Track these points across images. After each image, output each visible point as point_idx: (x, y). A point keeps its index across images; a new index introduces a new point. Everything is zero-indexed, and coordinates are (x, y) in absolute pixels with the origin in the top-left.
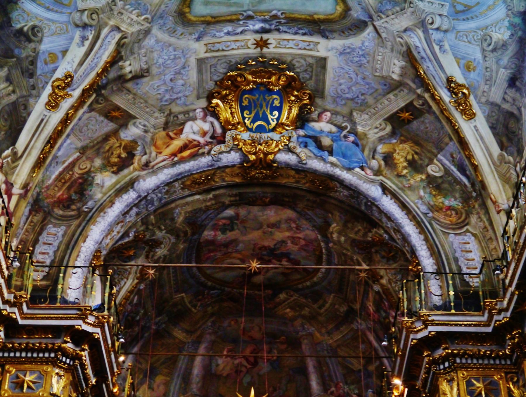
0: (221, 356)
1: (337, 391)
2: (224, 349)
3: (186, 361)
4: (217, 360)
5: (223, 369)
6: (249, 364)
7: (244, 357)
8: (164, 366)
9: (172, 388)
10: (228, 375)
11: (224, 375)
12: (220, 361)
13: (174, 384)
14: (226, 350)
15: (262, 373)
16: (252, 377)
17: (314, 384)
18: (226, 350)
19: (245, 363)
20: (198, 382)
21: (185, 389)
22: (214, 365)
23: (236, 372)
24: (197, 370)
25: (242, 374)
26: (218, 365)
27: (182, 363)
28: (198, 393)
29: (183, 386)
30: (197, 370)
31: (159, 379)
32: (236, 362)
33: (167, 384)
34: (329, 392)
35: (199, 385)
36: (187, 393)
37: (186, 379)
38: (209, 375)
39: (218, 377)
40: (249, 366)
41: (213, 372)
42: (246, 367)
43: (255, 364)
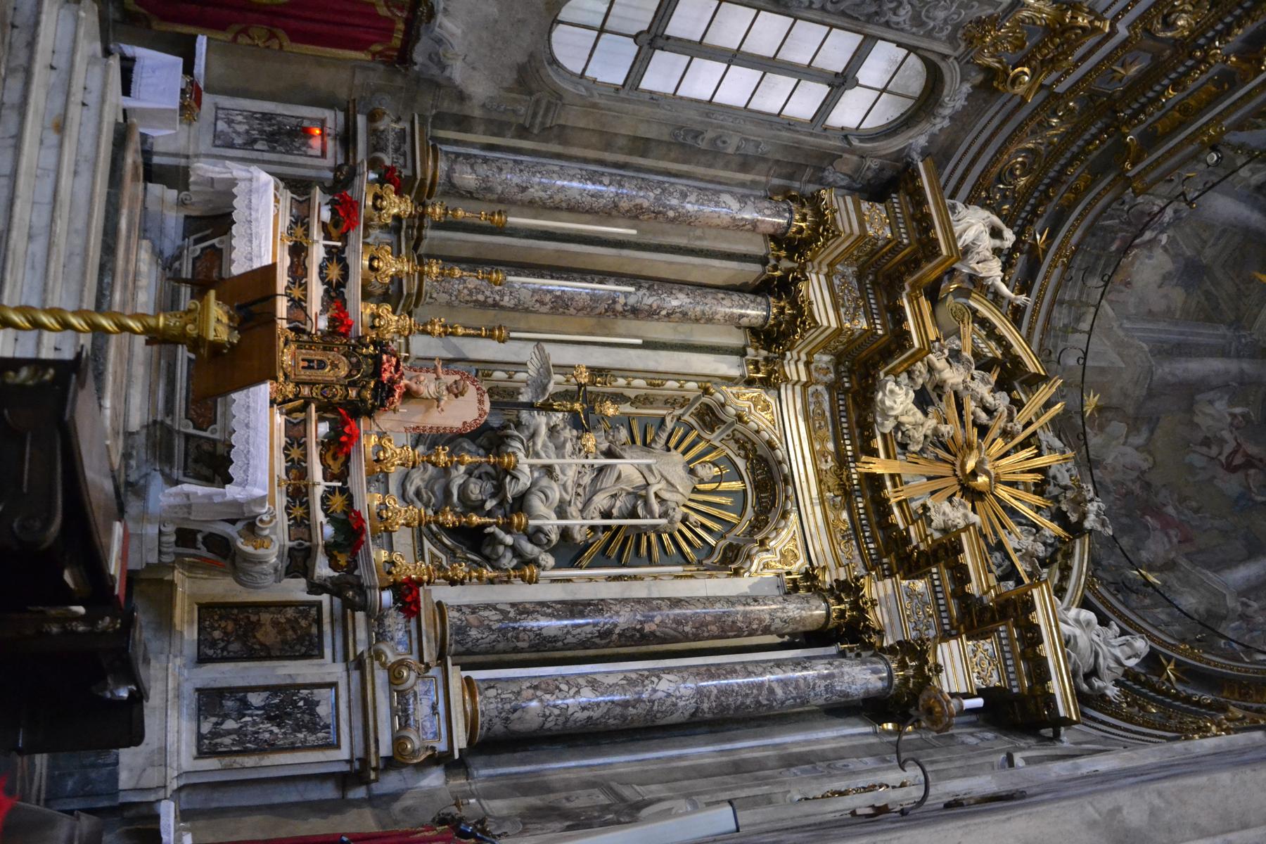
0: (1231, 403)
1: (1255, 612)
2: (1247, 405)
3: (1212, 341)
4: (1221, 398)
5: (1205, 414)
6: (1227, 457)
7: (1239, 445)
8: (1203, 298)
9: (1162, 326)
10: (1197, 425)
11: (1196, 419)
12: (1221, 406)
13: (1171, 328)
14: (1246, 410)
15: (1218, 483)
16: (1203, 468)
17: (1242, 574)
18: (1246, 410)
19: (1227, 450)
20: (1174, 375)
21: (1159, 352)
22: (1211, 395)
23: (1207, 438)
24: (1196, 367)
25: (1204, 450)
26: (1211, 402)
27: (1208, 334)
28: (1155, 378)
29: (1166, 346)
30: (1196, 367)
31: (1177, 295)
32: (1226, 434)
33: (1168, 314)
34: (1244, 599)
35: (1169, 378)
36: (1154, 356)
37: (1180, 350)
38: (1189, 392)
39: (1190, 409)
40: (1223, 458)
41: (1198, 397)
42: (1220, 454)
43: (1230, 468)
